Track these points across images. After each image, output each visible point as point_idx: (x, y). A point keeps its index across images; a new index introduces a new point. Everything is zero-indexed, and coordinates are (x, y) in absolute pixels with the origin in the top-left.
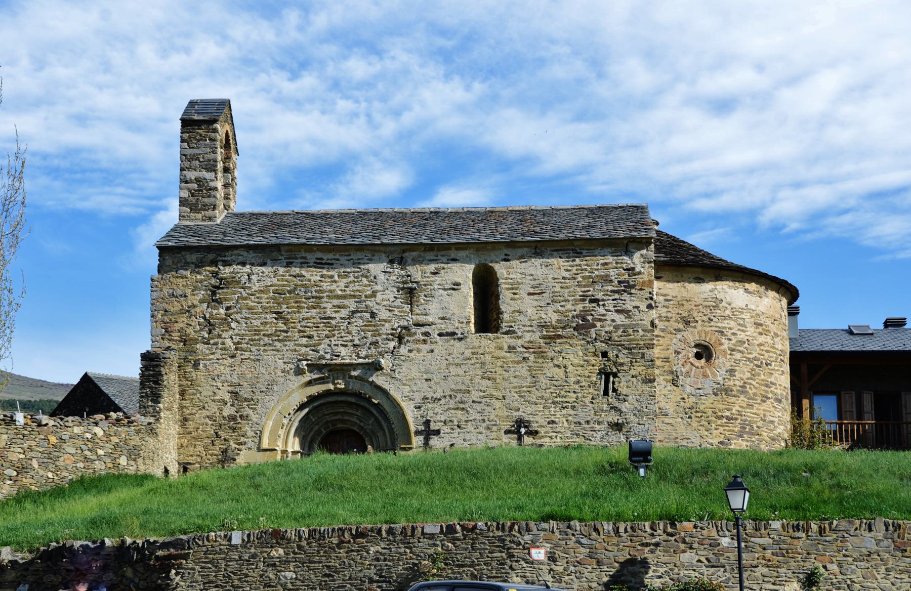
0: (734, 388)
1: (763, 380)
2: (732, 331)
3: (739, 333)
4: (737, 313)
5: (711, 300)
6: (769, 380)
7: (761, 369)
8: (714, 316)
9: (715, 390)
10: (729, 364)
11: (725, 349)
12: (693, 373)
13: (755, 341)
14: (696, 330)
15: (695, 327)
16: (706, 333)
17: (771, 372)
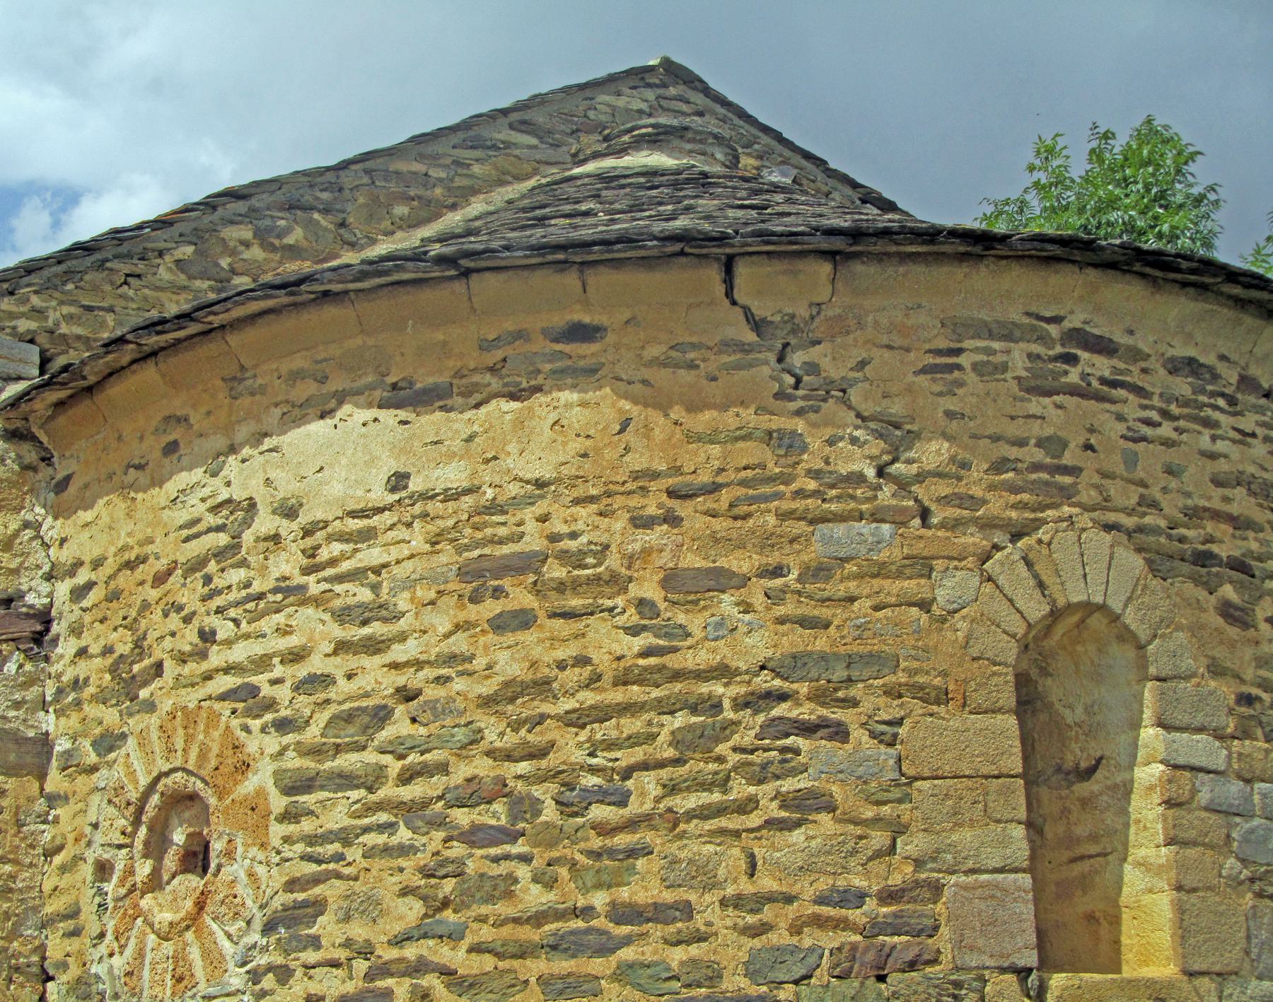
1: (538, 919)
2: (302, 671)
3: (337, 667)
4: (337, 548)
5: (212, 520)
6: (600, 900)
7: (519, 848)
8: (219, 611)
10: (278, 878)
11: (261, 793)
12: (146, 973)
13: (459, 685)
14: (154, 720)
15: (150, 707)
16: (190, 718)
17: (622, 840)
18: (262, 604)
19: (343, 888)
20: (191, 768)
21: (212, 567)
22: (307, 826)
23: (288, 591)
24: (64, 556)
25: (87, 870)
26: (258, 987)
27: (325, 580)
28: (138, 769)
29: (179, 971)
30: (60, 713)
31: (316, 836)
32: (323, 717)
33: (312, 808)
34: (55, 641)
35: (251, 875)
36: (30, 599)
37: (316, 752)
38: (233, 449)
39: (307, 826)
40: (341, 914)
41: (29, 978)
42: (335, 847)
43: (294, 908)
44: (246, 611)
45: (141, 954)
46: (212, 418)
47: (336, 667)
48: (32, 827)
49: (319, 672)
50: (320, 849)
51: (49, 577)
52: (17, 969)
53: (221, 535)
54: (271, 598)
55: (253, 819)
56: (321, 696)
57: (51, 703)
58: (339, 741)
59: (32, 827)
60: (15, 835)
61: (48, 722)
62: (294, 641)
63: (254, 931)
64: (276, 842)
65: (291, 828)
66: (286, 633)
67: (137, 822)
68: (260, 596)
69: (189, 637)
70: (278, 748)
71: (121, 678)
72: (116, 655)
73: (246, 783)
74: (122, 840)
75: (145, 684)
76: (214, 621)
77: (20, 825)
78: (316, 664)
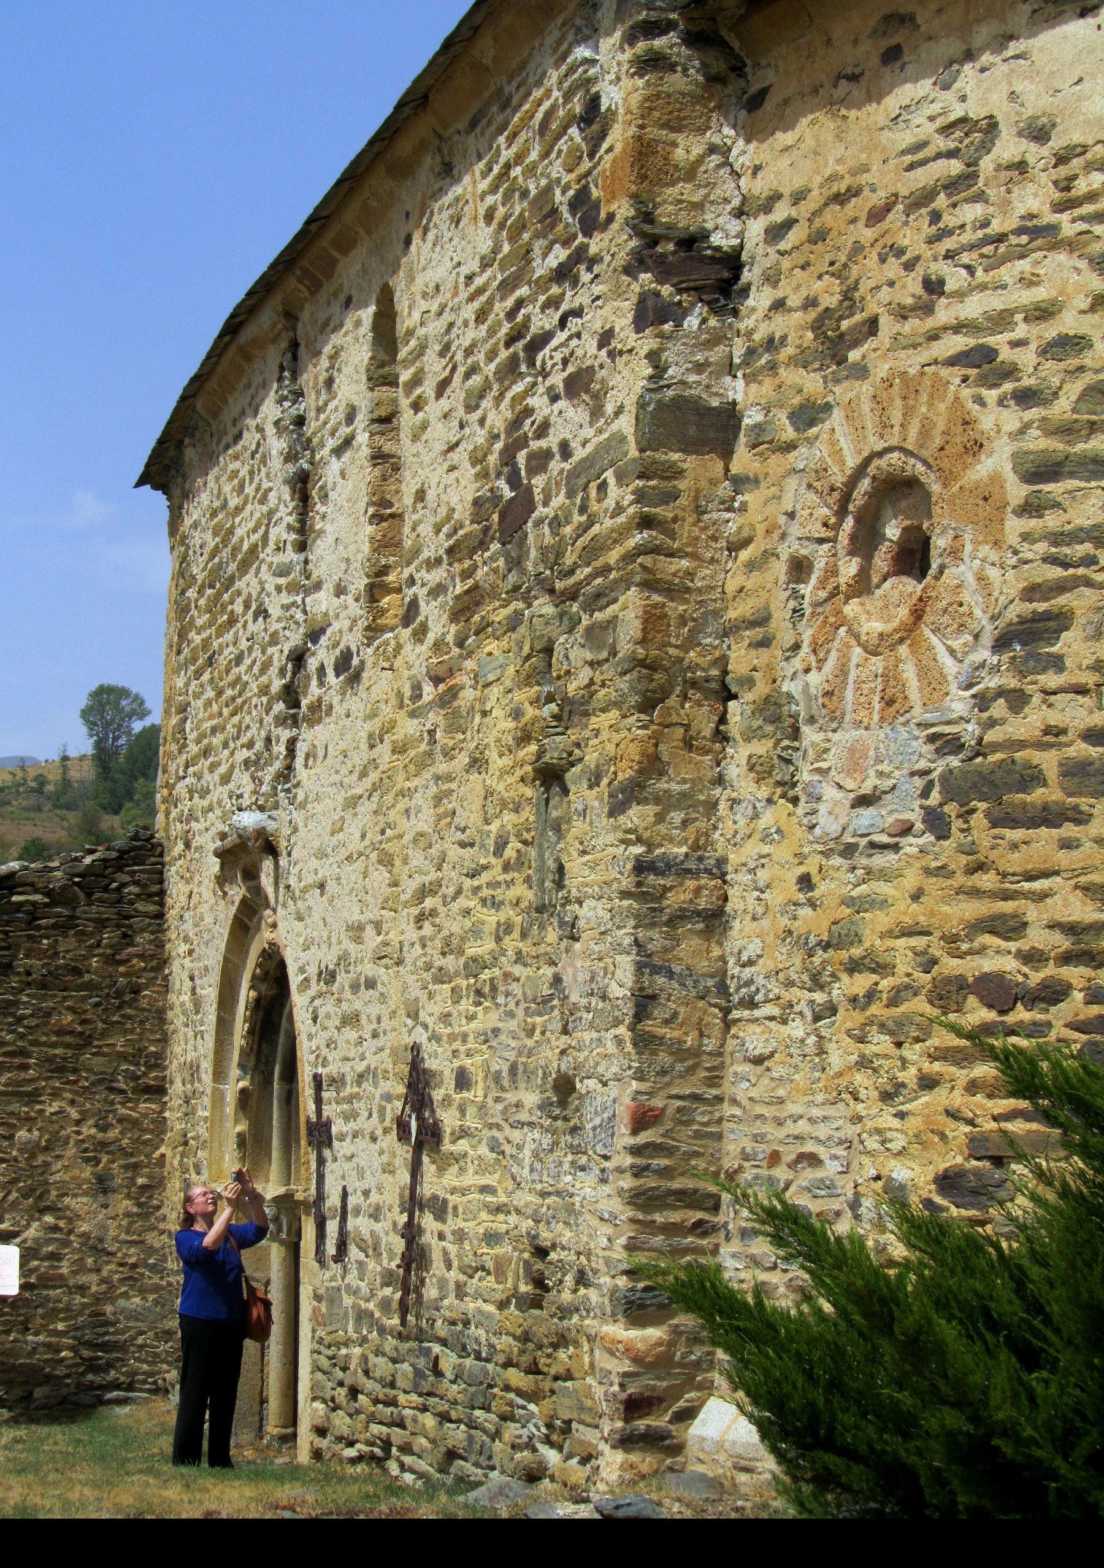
0: (1048, 761)
2: (1051, 331)
5: (942, 143)
8: (949, 256)
9: (935, 798)
11: (996, 479)
12: (849, 694)
14: (866, 388)
15: (861, 372)
16: (910, 387)
18: (1002, 248)
19: (1094, 598)
20: (910, 448)
21: (941, 201)
22: (1052, 521)
23: (1035, 232)
24: (759, 187)
25: (780, 569)
26: (985, 715)
27: (1082, 218)
28: (845, 447)
29: (890, 692)
30: (749, 379)
31: (1062, 534)
32: (1075, 389)
33: (1059, 499)
34: (745, 292)
35: (981, 578)
36: (716, 239)
37: (1066, 430)
38: (969, 56)
39: (1052, 521)
40: (1090, 630)
41: (707, 693)
42: (1084, 549)
43: (1033, 620)
44: (982, 256)
45: (843, 671)
46: (944, 17)
47: (1093, 326)
48: (715, 515)
49: (1071, 333)
50: (1067, 550)
51: (739, 213)
52: (694, 684)
53: (953, 161)
54: (1013, 240)
55: (987, 509)
56: (1073, 362)
57: (739, 367)
58: (1094, 418)
59: (715, 515)
60: (694, 525)
61: (736, 389)
62: (1041, 294)
63: (983, 647)
64: (1013, 539)
65: (1033, 523)
66: (1032, 284)
67: (842, 512)
68: (1001, 238)
69: (912, 287)
70: (1017, 425)
71: (826, 337)
72: (821, 308)
73: (978, 467)
74: (824, 533)
75: (856, 344)
76: (943, 268)
77: (700, 511)
78: (1068, 323)
